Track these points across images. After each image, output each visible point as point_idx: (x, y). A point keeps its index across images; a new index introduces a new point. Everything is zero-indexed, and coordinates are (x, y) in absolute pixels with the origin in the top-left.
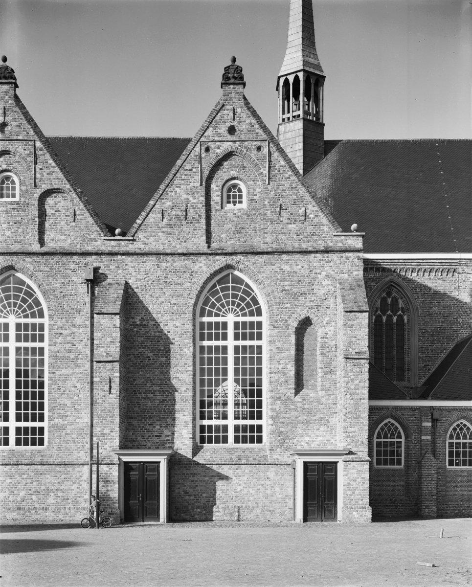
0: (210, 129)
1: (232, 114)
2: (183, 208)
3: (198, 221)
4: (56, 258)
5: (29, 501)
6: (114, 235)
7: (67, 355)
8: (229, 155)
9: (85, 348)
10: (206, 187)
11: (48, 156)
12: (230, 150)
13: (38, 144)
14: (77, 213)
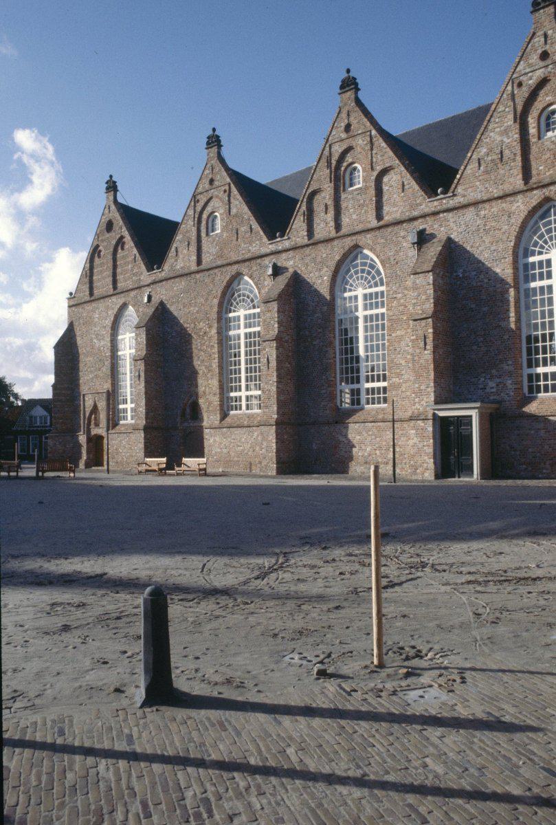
0: (522, 63)
1: (543, 39)
2: (498, 151)
3: (514, 160)
4: (390, 229)
5: (374, 456)
6: (437, 195)
8: (543, 82)
10: (520, 123)
11: (381, 140)
12: (543, 76)
13: (374, 132)
14: (405, 183)
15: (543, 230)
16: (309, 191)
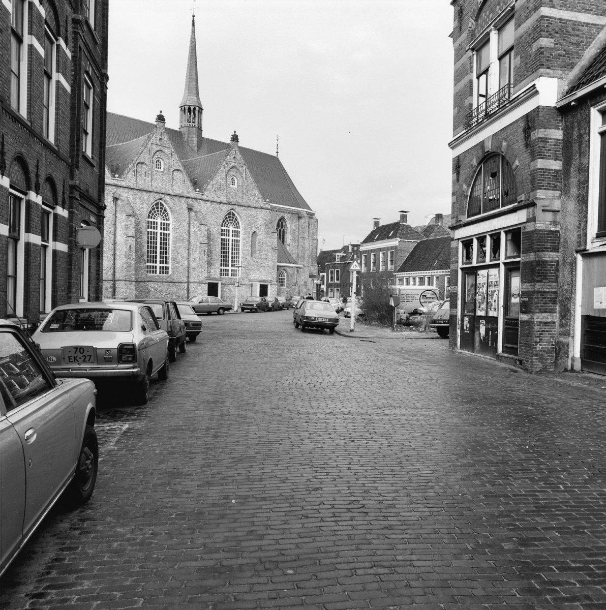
11: (176, 156)
16: (138, 161)
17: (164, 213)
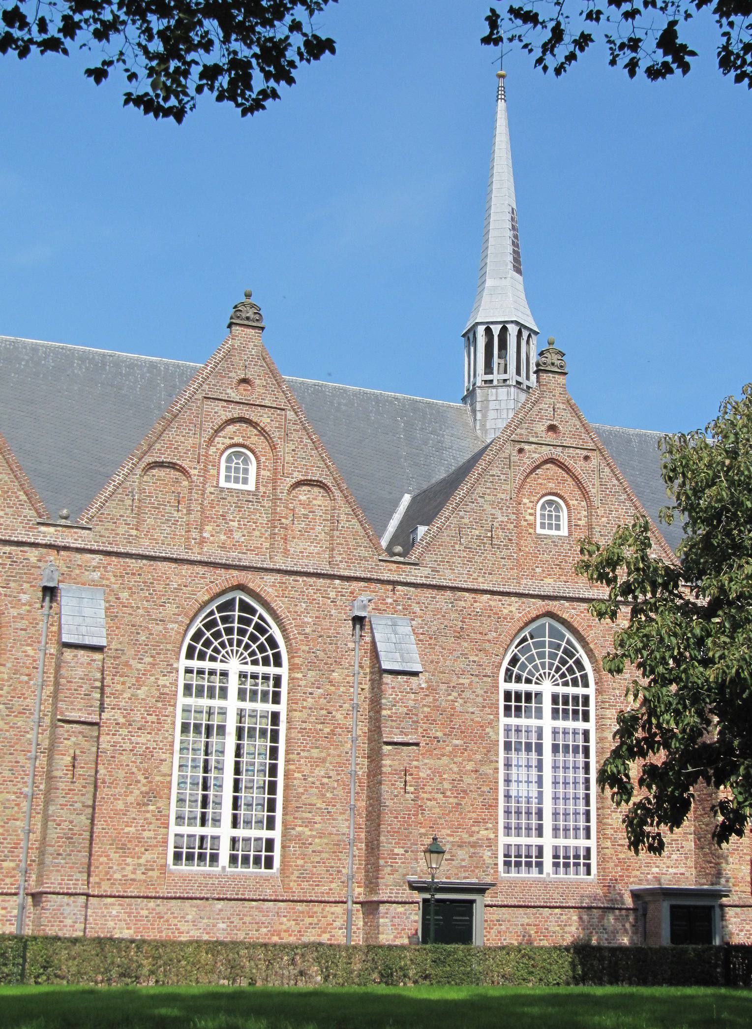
7: (320, 726)
9: (345, 718)
15: (534, 651)
17: (254, 638)
